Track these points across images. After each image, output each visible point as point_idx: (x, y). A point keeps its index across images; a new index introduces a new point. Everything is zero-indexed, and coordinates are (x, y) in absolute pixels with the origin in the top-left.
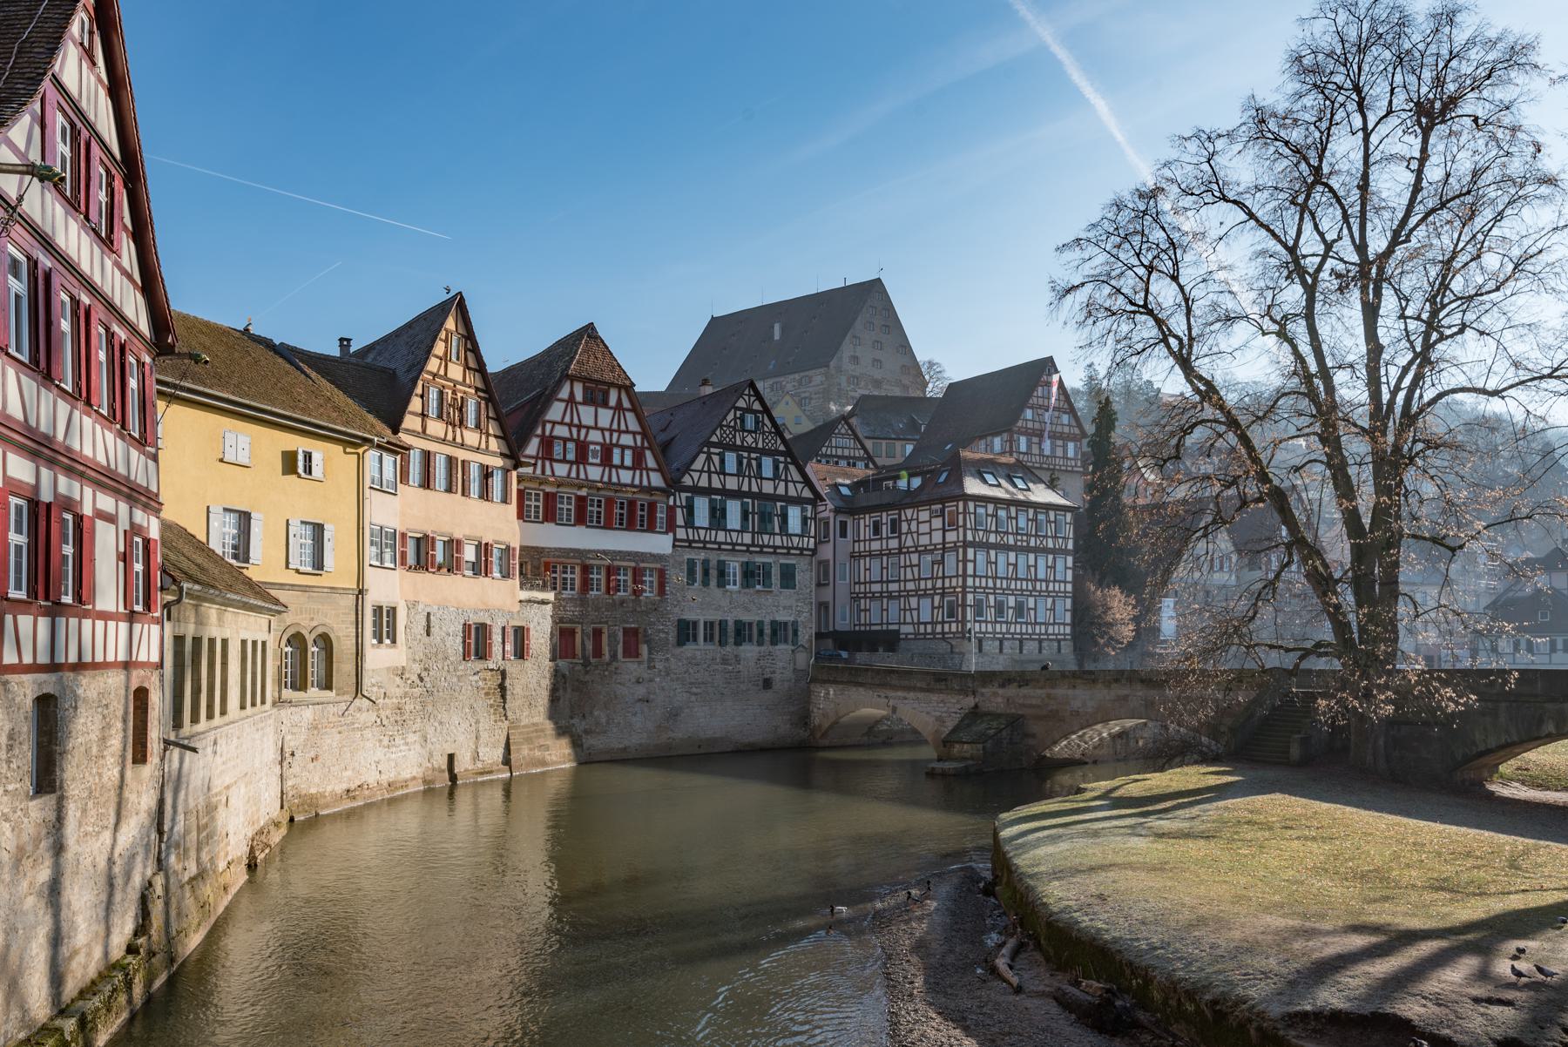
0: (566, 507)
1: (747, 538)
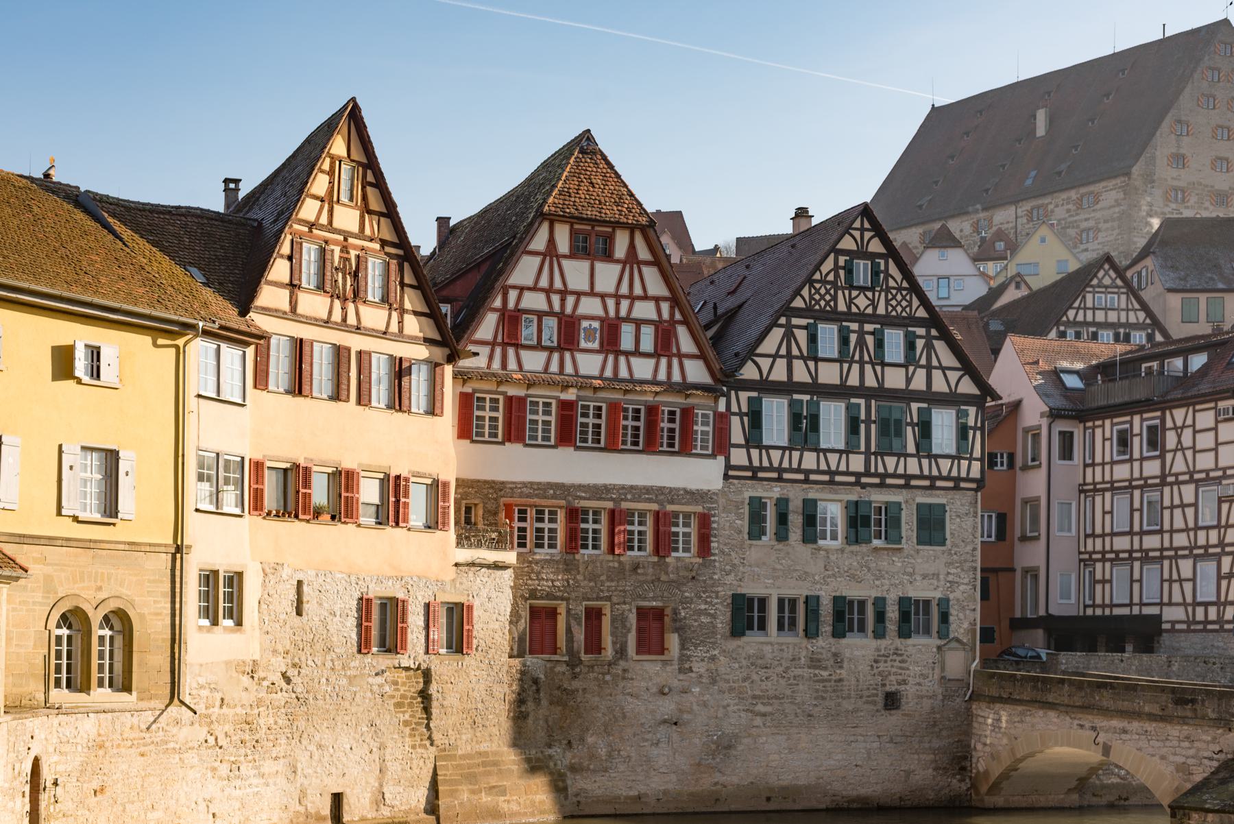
0: (544, 419)
1: (857, 463)
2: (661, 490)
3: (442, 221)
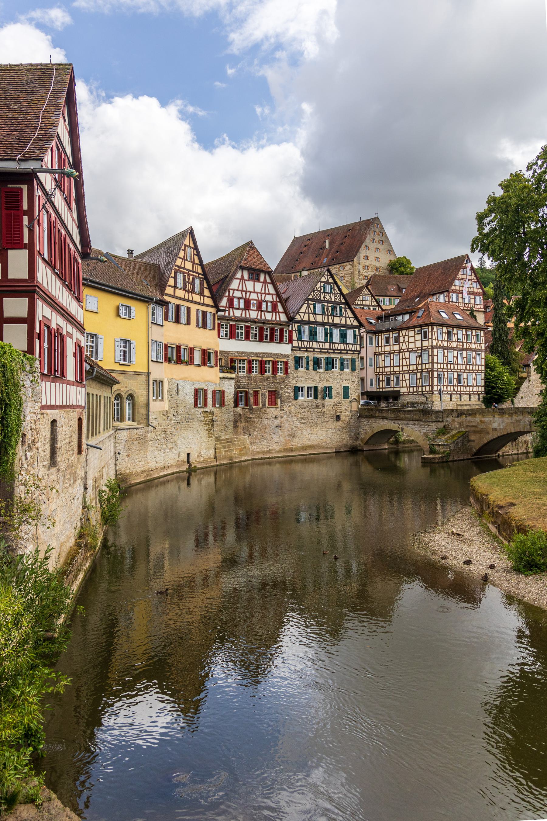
2: (274, 354)
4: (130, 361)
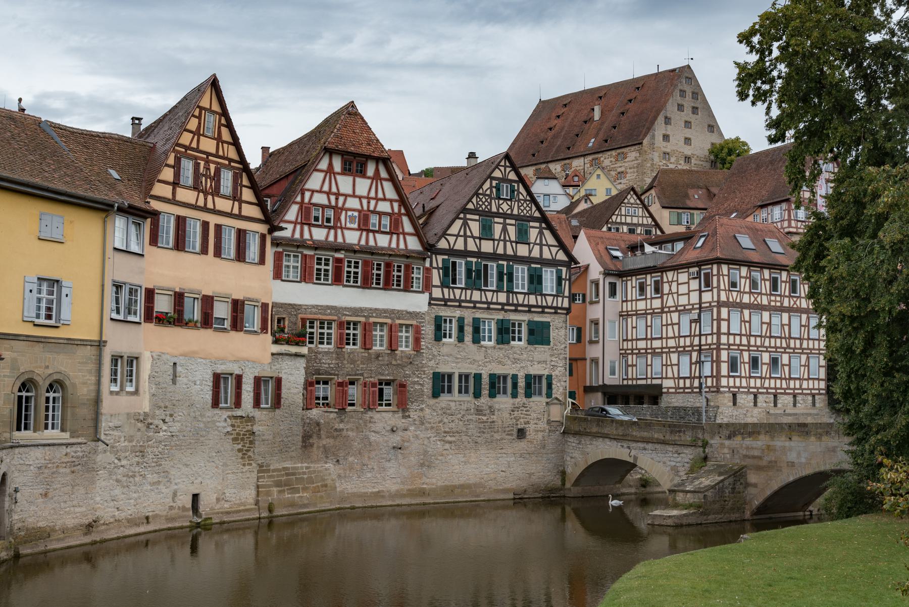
2: (393, 311)
3: (265, 149)
4: (58, 319)
